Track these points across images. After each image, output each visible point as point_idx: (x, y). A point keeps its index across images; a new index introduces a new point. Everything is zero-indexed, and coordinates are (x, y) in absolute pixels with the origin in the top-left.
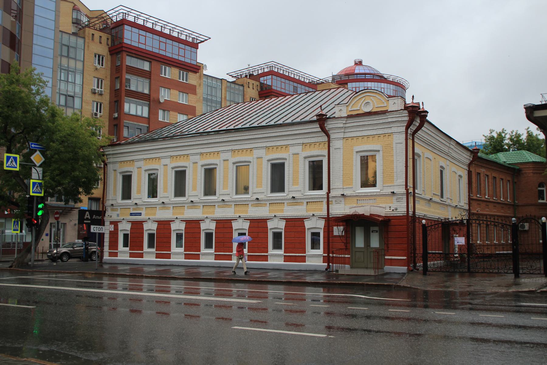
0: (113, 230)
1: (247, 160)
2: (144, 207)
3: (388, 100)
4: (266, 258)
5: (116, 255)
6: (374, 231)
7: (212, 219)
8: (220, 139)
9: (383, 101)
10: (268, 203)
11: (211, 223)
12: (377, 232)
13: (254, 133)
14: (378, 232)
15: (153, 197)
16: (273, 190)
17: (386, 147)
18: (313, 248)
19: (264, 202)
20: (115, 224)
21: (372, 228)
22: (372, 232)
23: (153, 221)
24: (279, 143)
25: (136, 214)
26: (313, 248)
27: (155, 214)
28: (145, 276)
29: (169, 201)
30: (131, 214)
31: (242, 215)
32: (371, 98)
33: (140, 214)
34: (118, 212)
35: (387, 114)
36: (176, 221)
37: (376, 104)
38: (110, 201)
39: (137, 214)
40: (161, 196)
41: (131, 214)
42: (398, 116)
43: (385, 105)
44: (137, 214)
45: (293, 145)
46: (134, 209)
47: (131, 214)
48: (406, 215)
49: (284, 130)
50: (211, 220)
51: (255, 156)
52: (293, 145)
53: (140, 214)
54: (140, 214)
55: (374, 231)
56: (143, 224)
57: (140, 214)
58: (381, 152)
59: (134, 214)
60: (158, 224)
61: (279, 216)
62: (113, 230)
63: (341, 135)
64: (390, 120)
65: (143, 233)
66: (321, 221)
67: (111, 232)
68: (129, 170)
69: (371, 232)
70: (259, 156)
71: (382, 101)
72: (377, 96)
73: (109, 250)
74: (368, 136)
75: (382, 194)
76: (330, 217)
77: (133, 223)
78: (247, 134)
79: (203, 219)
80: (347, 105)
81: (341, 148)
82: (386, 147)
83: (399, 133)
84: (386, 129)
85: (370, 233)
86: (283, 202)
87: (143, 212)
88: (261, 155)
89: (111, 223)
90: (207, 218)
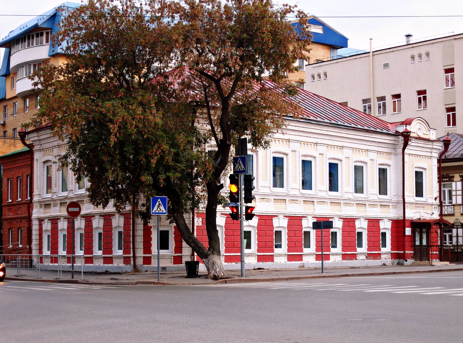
7: (313, 216)
19: (352, 202)
32: (421, 125)
42: (438, 145)
51: (345, 155)
64: (434, 147)
73: (144, 253)
76: (406, 219)
86: (365, 203)
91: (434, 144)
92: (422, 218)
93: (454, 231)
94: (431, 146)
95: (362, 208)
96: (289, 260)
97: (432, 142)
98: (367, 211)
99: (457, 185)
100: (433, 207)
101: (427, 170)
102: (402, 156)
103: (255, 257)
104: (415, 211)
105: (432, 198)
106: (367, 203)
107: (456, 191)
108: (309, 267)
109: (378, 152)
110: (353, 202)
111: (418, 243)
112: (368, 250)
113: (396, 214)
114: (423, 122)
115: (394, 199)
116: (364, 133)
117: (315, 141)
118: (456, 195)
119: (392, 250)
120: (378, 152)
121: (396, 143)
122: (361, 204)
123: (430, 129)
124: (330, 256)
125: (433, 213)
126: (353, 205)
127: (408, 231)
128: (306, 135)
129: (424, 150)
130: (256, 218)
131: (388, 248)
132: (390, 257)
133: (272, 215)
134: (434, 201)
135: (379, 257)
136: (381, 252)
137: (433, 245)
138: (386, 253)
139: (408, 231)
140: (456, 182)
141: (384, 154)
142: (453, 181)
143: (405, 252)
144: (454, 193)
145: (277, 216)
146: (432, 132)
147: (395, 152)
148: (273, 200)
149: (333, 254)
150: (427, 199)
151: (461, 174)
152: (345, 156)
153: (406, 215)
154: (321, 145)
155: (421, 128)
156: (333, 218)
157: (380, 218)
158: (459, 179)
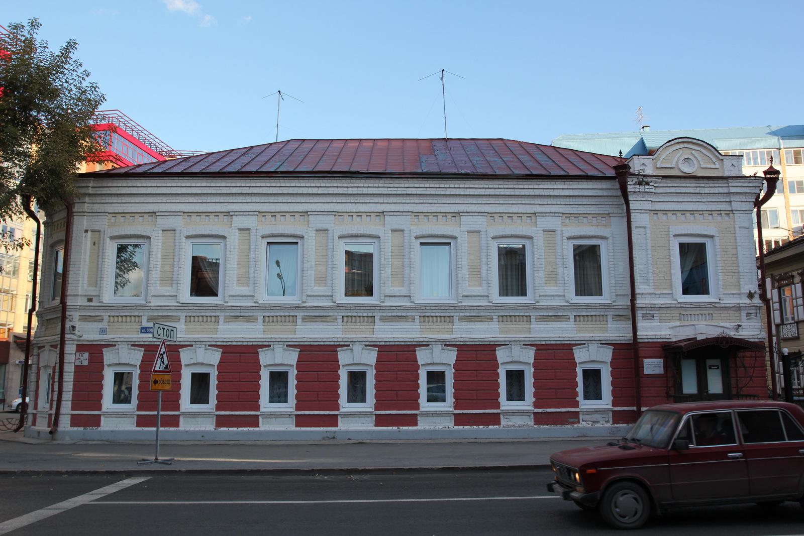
0: (85, 363)
1: (448, 233)
2: (182, 315)
3: (722, 160)
5: (95, 421)
6: (713, 366)
7: (368, 343)
8: (389, 189)
9: (714, 159)
12: (718, 368)
14: (720, 367)
16: (505, 291)
17: (723, 232)
20: (95, 351)
21: (710, 362)
22: (710, 368)
23: (209, 345)
24: (514, 209)
32: (694, 152)
34: (104, 325)
37: (701, 163)
38: (79, 298)
40: (310, 293)
42: (746, 185)
45: (544, 214)
47: (142, 328)
48: (632, 342)
50: (366, 345)
51: (465, 228)
55: (713, 366)
62: (85, 363)
63: (648, 206)
64: (732, 190)
66: (605, 349)
67: (78, 369)
69: (708, 367)
71: (711, 159)
72: (703, 151)
74: (692, 212)
75: (723, 305)
76: (638, 341)
77: (150, 351)
81: (648, 226)
82: (723, 232)
83: (743, 212)
84: (721, 203)
85: (706, 369)
89: (81, 348)
91: (730, 184)
92: (699, 338)
96: (377, 424)
97: (725, 181)
100: (743, 313)
101: (717, 240)
103: (213, 417)
104: (678, 323)
105: (739, 294)
108: (349, 439)
109: (568, 216)
110: (492, 314)
112: (536, 405)
113: (619, 331)
114: (705, 147)
116: (515, 183)
117: (380, 208)
119: (614, 404)
120: (568, 216)
122: (508, 317)
124: (419, 418)
125: (739, 326)
126: (492, 319)
127: (652, 366)
128: (352, 199)
130: (217, 351)
131: (606, 401)
132: (611, 419)
134: (748, 301)
135: (571, 420)
136: (577, 410)
137: (742, 393)
138: (596, 411)
139: (652, 366)
143: (639, 409)
145: (270, 346)
147: (620, 212)
148: (261, 319)
149: (427, 414)
150: (721, 296)
153: (638, 333)
154: (395, 214)
155: (690, 157)
156: (428, 345)
157: (574, 342)
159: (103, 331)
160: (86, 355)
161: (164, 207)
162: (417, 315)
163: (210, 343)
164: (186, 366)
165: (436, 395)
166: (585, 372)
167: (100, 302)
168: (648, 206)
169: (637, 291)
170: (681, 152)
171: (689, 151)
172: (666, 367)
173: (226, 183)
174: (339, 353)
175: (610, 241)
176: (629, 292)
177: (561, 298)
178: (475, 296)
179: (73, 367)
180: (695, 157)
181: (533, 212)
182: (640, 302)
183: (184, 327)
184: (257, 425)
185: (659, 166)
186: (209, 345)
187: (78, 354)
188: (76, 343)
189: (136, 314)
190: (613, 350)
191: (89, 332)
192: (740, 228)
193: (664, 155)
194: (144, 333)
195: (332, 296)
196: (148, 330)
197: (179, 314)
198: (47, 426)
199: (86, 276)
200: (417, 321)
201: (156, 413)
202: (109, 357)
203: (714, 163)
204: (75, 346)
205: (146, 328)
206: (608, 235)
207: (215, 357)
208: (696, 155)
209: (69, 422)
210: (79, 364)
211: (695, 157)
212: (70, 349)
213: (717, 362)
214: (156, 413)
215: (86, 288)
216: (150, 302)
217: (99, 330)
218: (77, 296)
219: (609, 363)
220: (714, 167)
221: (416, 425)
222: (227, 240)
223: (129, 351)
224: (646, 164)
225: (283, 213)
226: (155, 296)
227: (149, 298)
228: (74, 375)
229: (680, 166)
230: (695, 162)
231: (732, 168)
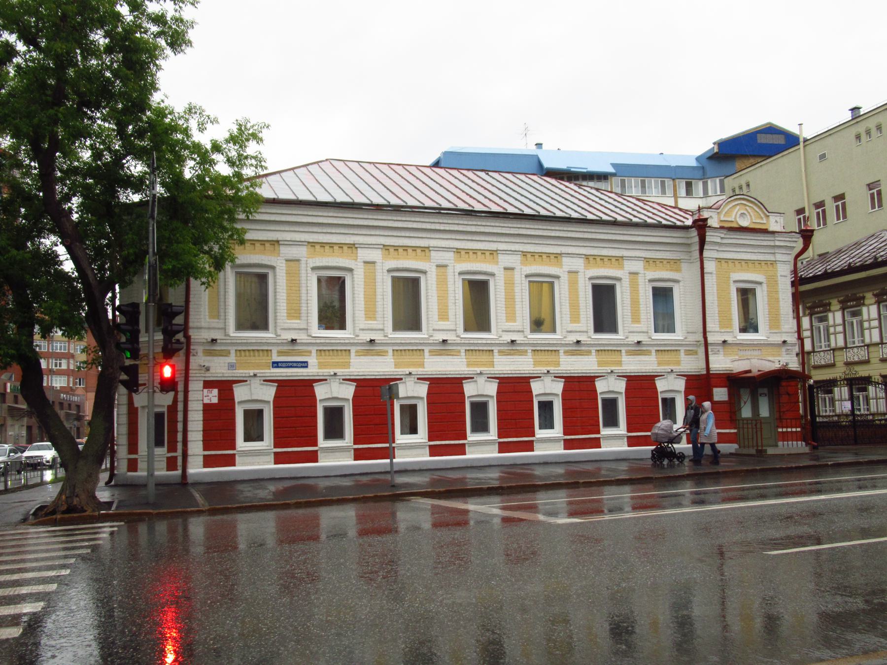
0: (215, 400)
2: (314, 349)
4: (313, 457)
7: (489, 376)
9: (762, 215)
10: (463, 349)
11: (488, 384)
13: (545, 227)
15: (254, 327)
18: (248, 438)
20: (225, 387)
21: (760, 391)
23: (343, 380)
24: (605, 252)
25: (290, 364)
26: (248, 438)
27: (347, 365)
28: (583, 483)
29: (383, 338)
30: (276, 365)
31: (552, 369)
32: (747, 208)
33: (304, 365)
34: (232, 359)
35: (776, 235)
36: (407, 380)
37: (753, 217)
39: (295, 365)
41: (276, 365)
42: (788, 239)
43: (765, 222)
44: (295, 365)
45: (630, 258)
46: (280, 353)
47: (273, 363)
49: (613, 232)
51: (566, 268)
52: (630, 258)
53: (304, 365)
54: (304, 365)
56: (313, 387)
57: (304, 365)
58: (764, 286)
59: (284, 365)
60: (356, 386)
61: (261, 375)
62: (215, 400)
63: (715, 255)
64: (777, 243)
65: (315, 406)
67: (208, 409)
68: (264, 262)
70: (574, 268)
72: (755, 207)
74: (747, 261)
76: (711, 372)
78: (540, 227)
79: (245, 379)
80: (719, 211)
86: (619, 349)
87: (312, 360)
88: (576, 267)
89: (208, 385)
90: (481, 373)
93: (871, 389)
94: (772, 243)
95: (484, 357)
98: (495, 363)
99: (870, 311)
102: (698, 264)
106: (623, 349)
107: (869, 320)
109: (647, 260)
111: (746, 412)
113: (693, 365)
114: (752, 202)
115: (692, 338)
118: (870, 328)
121: (689, 242)
123: (768, 214)
129: (756, 251)
133: (231, 379)
140: (868, 306)
141: (665, 262)
142: (864, 304)
144: (866, 325)
146: (772, 219)
148: (390, 352)
151: (875, 292)
152: (567, 270)
153: (711, 366)
158: (873, 300)
159: (232, 366)
160: (215, 392)
161: (288, 236)
162: (529, 349)
163: (344, 378)
164: (320, 400)
165: (547, 423)
166: (604, 400)
167: (225, 335)
168: (715, 255)
169: (708, 329)
170: (738, 207)
171: (743, 207)
172: (730, 394)
173: (334, 212)
174: (464, 385)
175: (681, 284)
176: (701, 330)
177: (645, 334)
178: (576, 332)
179: (202, 405)
180: (749, 213)
181: (621, 255)
182: (711, 339)
183: (315, 360)
184: (316, 461)
185: (722, 218)
186: (343, 380)
187: (205, 391)
188: (203, 379)
189: (266, 348)
190: (499, 383)
191: (220, 369)
192: (781, 276)
193: (726, 209)
194: (276, 367)
195: (456, 330)
196: (280, 365)
197: (309, 348)
198: (165, 469)
199: (207, 307)
200: (530, 354)
201: (387, 445)
202: (240, 393)
203: (762, 218)
204: (202, 382)
205: (277, 363)
206: (680, 279)
207: (348, 392)
208: (749, 211)
209: (202, 463)
210: (208, 402)
211: (749, 213)
212: (196, 386)
213: (765, 391)
214: (387, 445)
215: (208, 320)
216: (280, 336)
217: (227, 365)
218: (201, 328)
219: (683, 393)
220: (762, 222)
221: (533, 450)
222: (355, 272)
223: (262, 387)
224: (713, 216)
225: (405, 248)
226: (363, 330)
227: (279, 332)
228: (204, 414)
229: (738, 219)
230: (749, 217)
231: (775, 224)
